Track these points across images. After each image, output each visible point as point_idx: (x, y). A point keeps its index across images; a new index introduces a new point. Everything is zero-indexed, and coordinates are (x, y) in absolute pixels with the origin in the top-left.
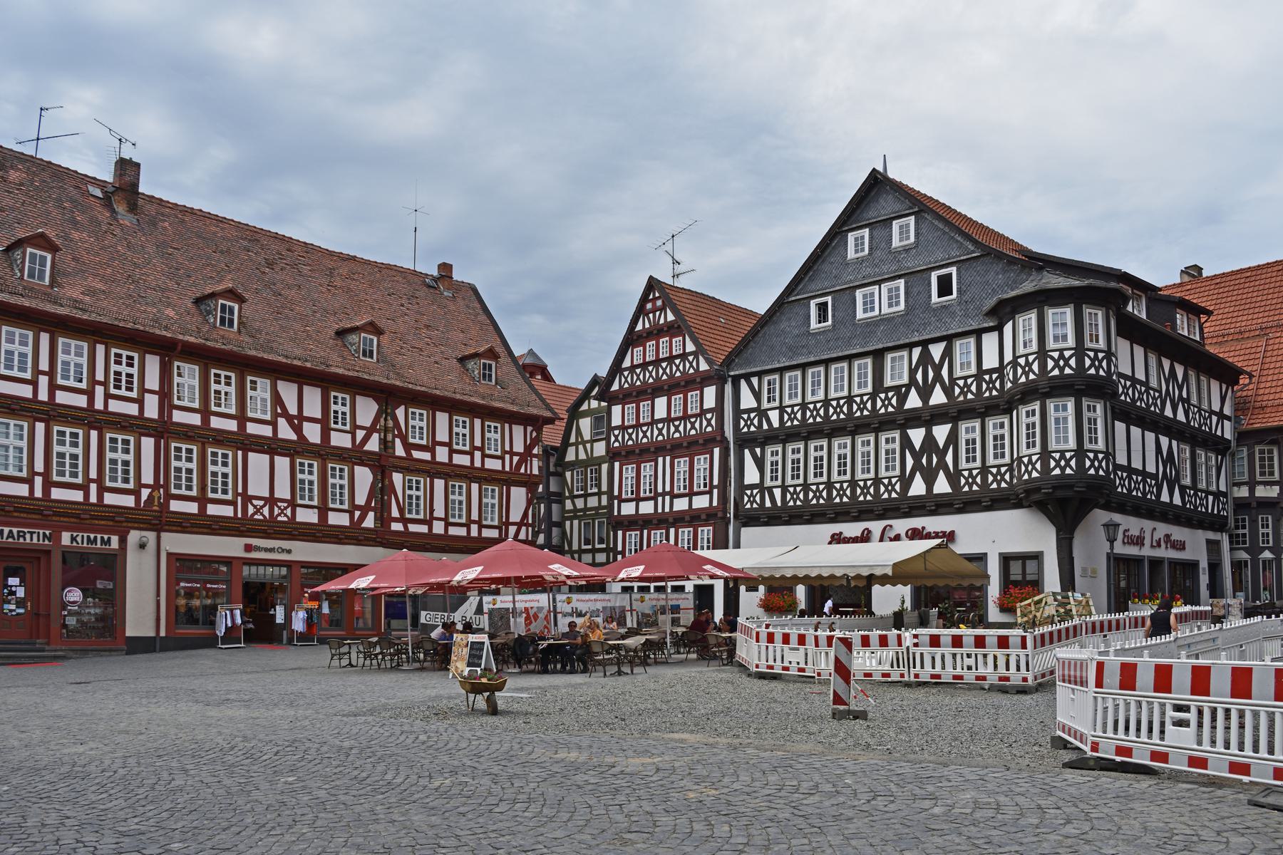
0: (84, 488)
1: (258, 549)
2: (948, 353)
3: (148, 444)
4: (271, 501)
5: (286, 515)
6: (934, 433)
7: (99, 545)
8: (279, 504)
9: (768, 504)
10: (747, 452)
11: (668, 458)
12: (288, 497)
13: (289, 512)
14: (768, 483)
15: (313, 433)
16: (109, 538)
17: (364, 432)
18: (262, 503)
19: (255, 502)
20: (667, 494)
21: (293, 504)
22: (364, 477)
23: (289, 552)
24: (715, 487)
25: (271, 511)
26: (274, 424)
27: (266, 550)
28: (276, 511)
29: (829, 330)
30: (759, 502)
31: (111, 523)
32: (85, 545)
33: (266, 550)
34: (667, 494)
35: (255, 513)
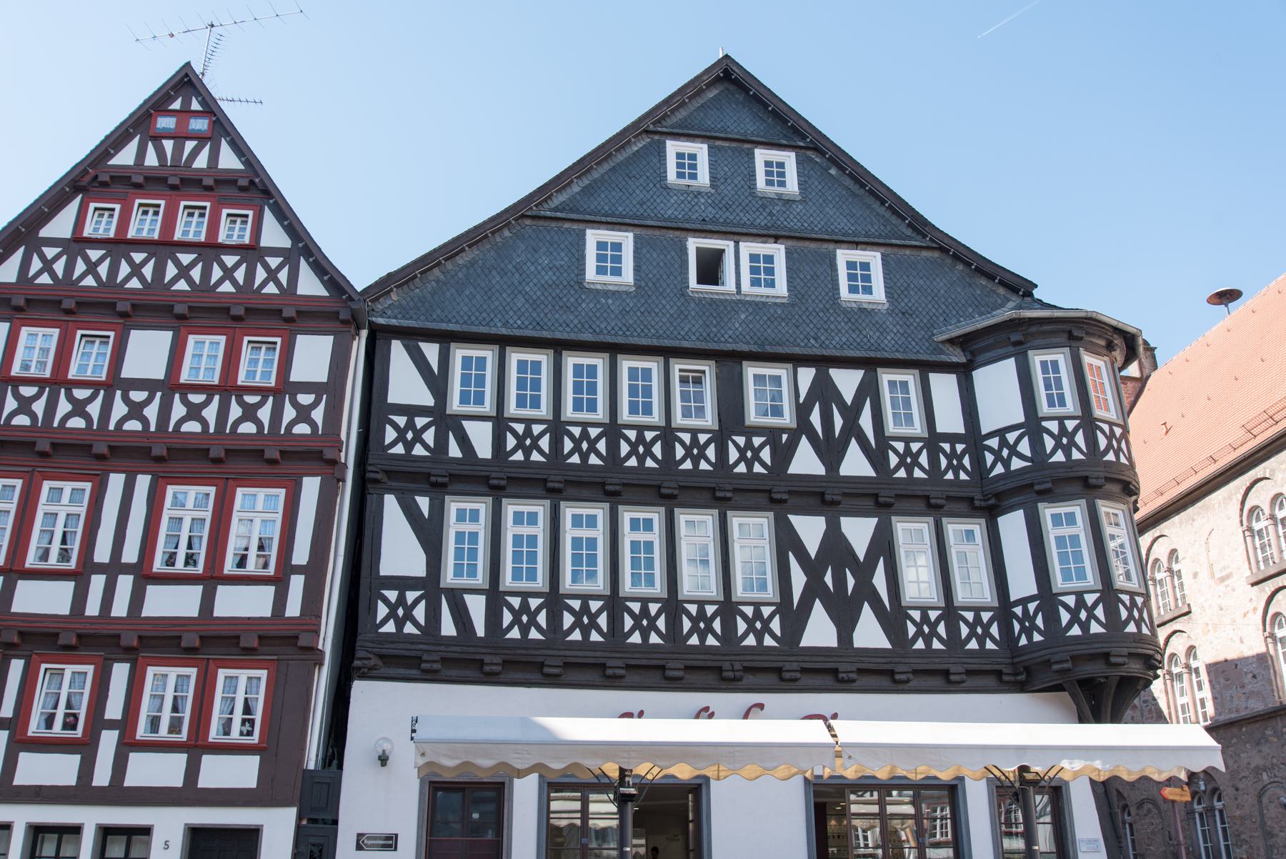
2: (869, 390)
6: (844, 530)
9: (448, 628)
10: (390, 502)
11: (143, 482)
14: (449, 578)
20: (127, 569)
24: (298, 570)
29: (628, 293)
34: (127, 569)
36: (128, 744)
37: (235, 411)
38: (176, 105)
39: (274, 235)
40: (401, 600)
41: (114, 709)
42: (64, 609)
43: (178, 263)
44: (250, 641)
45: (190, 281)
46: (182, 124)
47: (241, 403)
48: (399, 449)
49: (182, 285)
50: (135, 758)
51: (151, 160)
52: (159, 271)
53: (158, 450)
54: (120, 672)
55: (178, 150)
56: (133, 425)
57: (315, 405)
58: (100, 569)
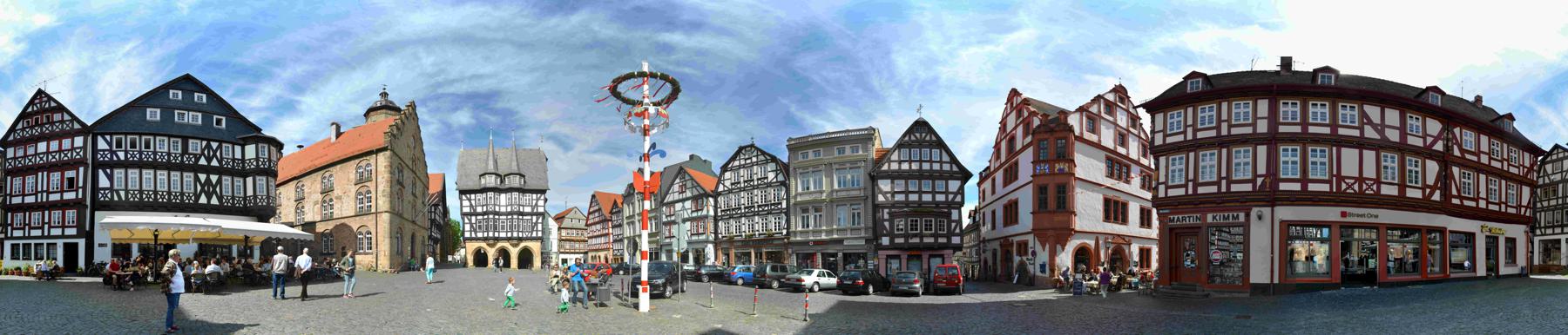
0: (1218, 183)
1: (1352, 215)
3: (1262, 150)
4: (1361, 179)
5: (1372, 190)
7: (1231, 220)
8: (1367, 182)
12: (1375, 177)
13: (1375, 187)
15: (1393, 136)
16: (1238, 215)
17: (1432, 139)
18: (1353, 181)
19: (1347, 181)
21: (1378, 181)
22: (1433, 167)
23: (1376, 216)
25: (1361, 186)
26: (1361, 129)
27: (1358, 216)
28: (1365, 187)
31: (1238, 204)
32: (1222, 221)
33: (1358, 216)
35: (1347, 189)
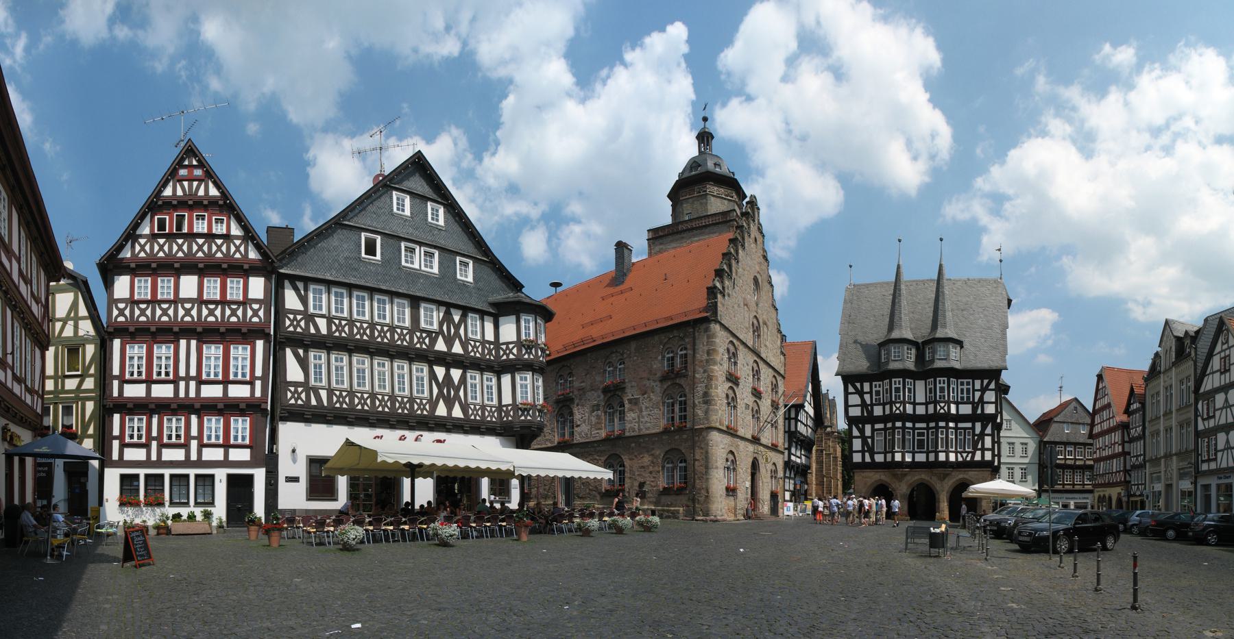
9: (314, 402)
10: (289, 352)
14: (312, 382)
20: (192, 378)
24: (258, 378)
30: (304, 399)
34: (192, 378)
36: (202, 446)
37: (228, 312)
38: (186, 163)
39: (236, 230)
40: (296, 391)
41: (194, 432)
42: (171, 395)
43: (197, 244)
44: (243, 406)
45: (204, 252)
46: (190, 173)
47: (230, 309)
48: (291, 329)
49: (200, 254)
50: (205, 450)
51: (180, 192)
52: (190, 247)
53: (199, 329)
54: (194, 419)
55: (190, 186)
56: (188, 319)
57: (259, 309)
58: (182, 379)
